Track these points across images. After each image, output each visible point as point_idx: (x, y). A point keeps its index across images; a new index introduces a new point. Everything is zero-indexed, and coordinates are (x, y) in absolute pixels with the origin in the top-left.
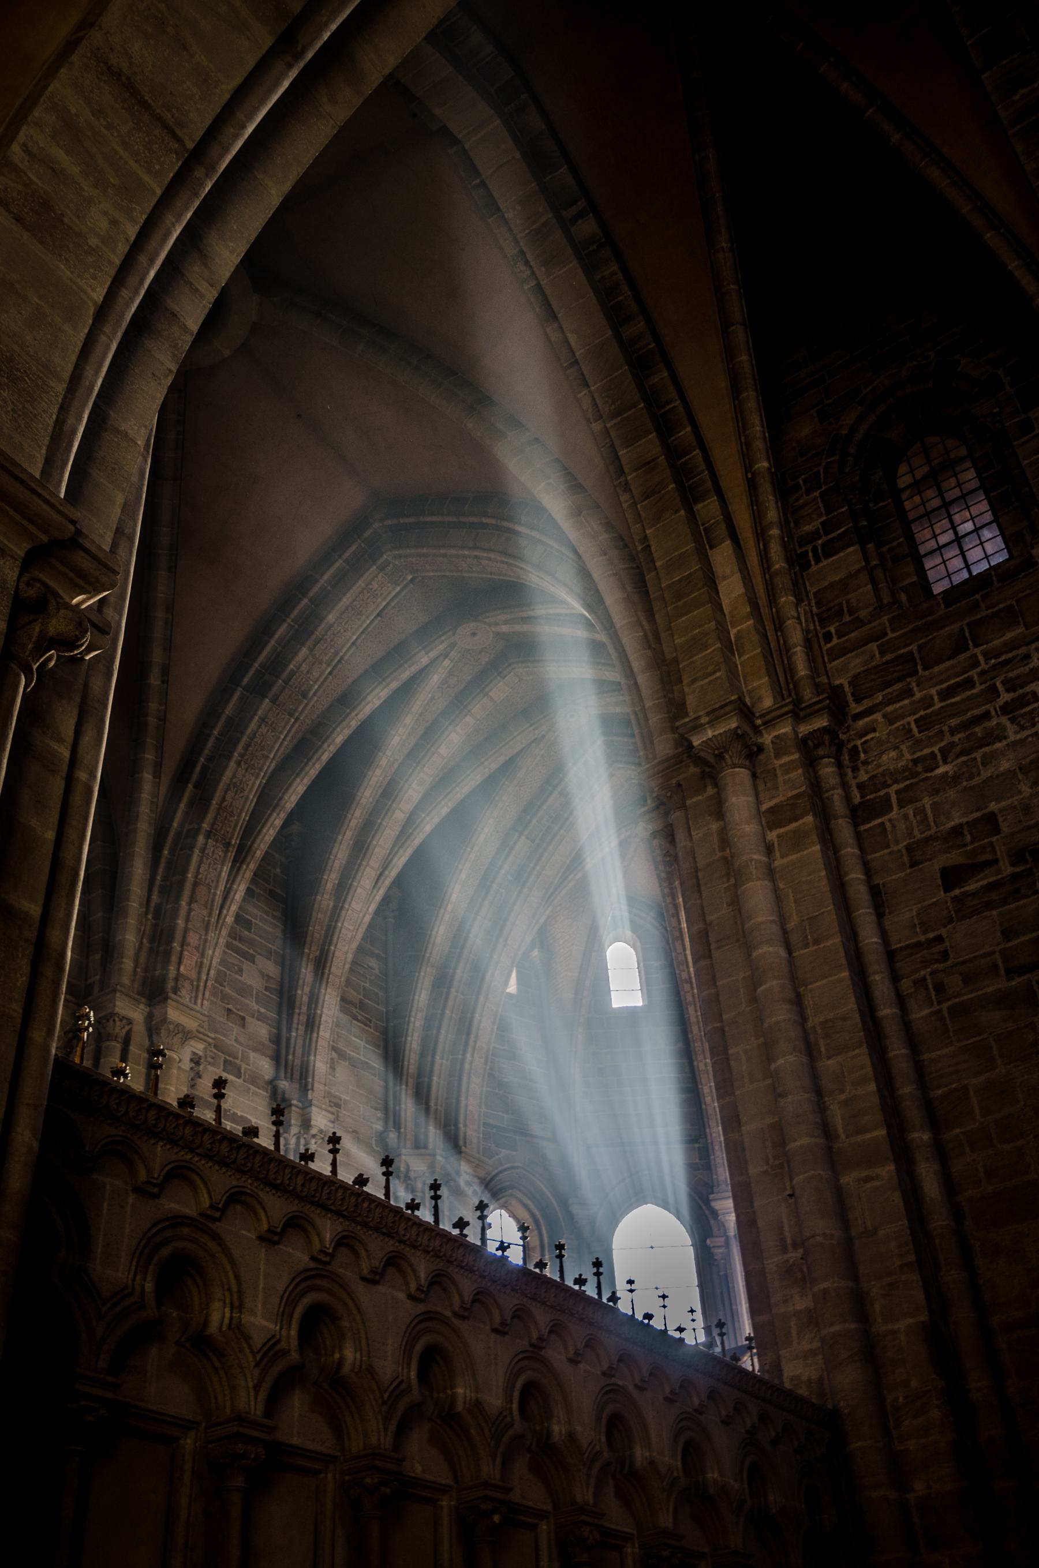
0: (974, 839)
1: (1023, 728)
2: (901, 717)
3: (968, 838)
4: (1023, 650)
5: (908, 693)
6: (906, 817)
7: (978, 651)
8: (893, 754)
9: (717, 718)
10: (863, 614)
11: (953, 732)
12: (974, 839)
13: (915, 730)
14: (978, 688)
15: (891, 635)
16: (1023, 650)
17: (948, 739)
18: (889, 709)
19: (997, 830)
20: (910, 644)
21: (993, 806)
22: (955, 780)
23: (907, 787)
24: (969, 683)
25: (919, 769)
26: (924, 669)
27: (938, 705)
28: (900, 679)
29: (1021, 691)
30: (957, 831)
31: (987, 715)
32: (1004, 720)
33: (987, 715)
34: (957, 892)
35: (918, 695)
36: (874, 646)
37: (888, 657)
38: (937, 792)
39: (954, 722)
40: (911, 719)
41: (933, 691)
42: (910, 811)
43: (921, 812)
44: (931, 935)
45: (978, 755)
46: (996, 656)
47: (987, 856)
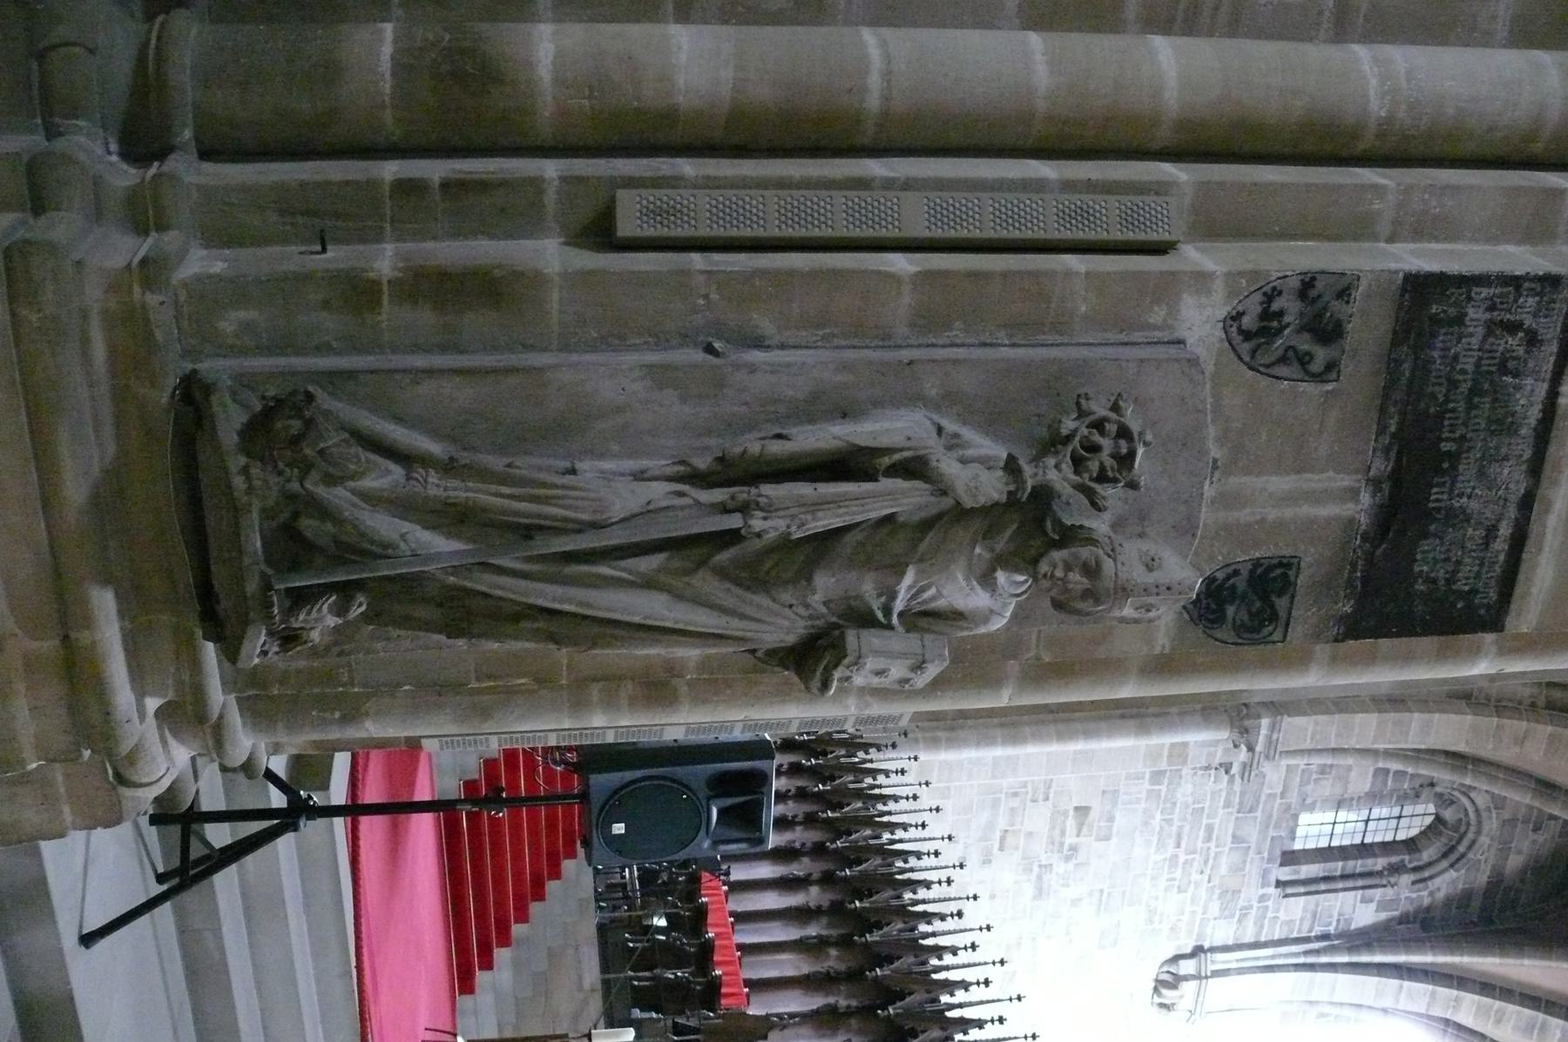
0: (1099, 828)
1: (1156, 863)
2: (1212, 799)
3: (1102, 824)
4: (1208, 871)
5: (1227, 805)
6: (1140, 793)
7: (1227, 849)
8: (1190, 791)
9: (1270, 742)
10: (1309, 788)
11: (1181, 827)
12: (1099, 828)
13: (1197, 806)
14: (1199, 844)
15: (1279, 801)
16: (1208, 871)
17: (1177, 823)
18: (1224, 794)
19: (1099, 839)
20: (1263, 811)
21: (1114, 840)
22: (1146, 823)
23: (1159, 796)
24: (1208, 839)
25: (1168, 805)
26: (1237, 818)
27: (1205, 821)
28: (1241, 803)
29: (1180, 865)
30: (1111, 819)
31: (1178, 845)
32: (1168, 855)
33: (1178, 845)
34: (1071, 813)
35: (1221, 811)
36: (1279, 790)
37: (1263, 797)
38: (1145, 811)
39: (1186, 829)
40: (1208, 804)
41: (1217, 821)
42: (1143, 795)
43: (1138, 801)
44: (1051, 796)
45: (1155, 839)
46: (1215, 859)
47: (1085, 830)
